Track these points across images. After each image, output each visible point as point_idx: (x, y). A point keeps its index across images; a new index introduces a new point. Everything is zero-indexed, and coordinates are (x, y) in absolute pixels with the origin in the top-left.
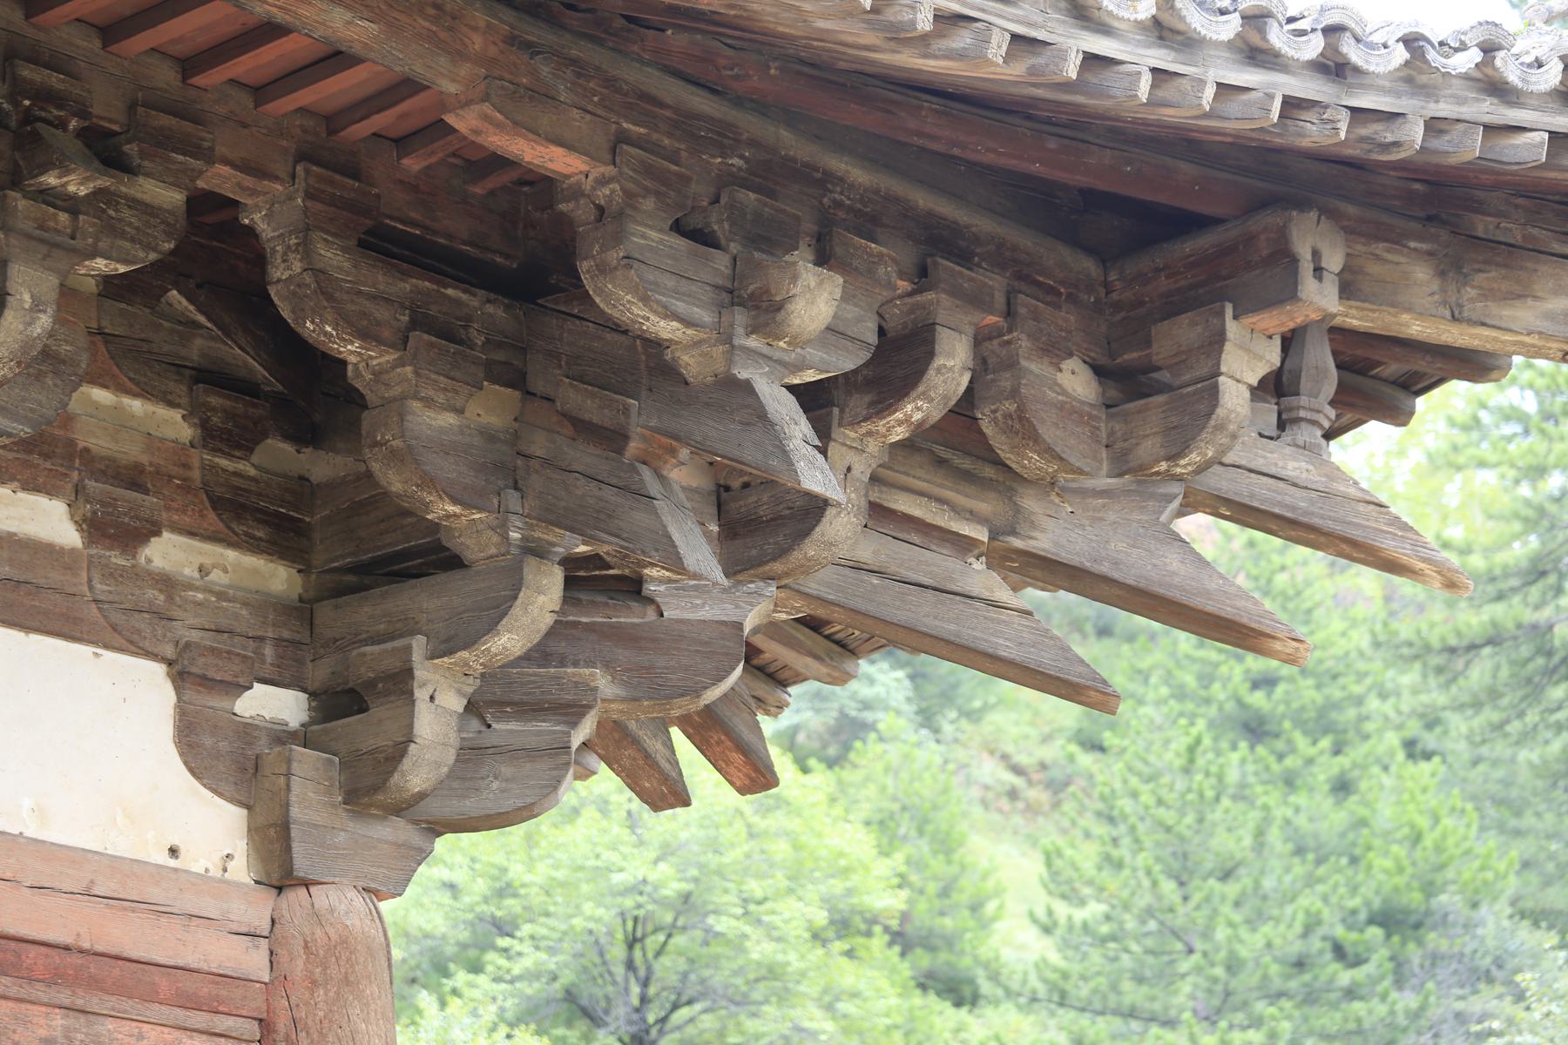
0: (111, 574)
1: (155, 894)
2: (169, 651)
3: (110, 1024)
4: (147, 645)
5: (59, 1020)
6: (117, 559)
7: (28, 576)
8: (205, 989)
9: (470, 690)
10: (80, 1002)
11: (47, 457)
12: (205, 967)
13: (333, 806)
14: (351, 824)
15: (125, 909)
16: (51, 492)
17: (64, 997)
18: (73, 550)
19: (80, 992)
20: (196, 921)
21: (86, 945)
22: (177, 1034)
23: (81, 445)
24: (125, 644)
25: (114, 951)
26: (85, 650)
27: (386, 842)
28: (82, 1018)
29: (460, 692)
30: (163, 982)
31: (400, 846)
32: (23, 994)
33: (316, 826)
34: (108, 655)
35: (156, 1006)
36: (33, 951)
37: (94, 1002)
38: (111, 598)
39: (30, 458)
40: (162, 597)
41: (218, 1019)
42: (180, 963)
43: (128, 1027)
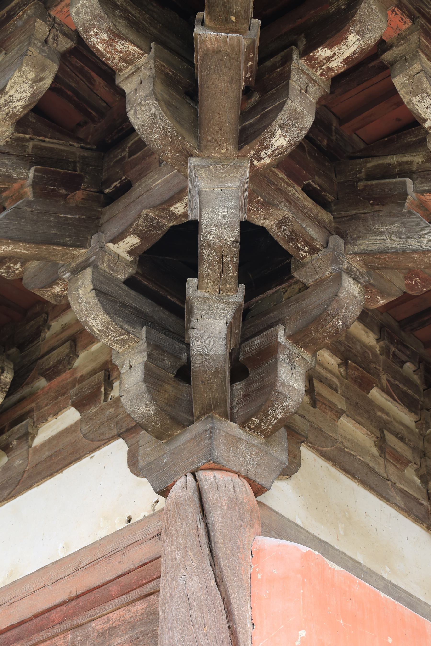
0: (91, 419)
1: (110, 547)
2: (115, 432)
3: (93, 624)
4: (107, 436)
5: (70, 636)
6: (93, 410)
7: (57, 449)
8: (133, 576)
9: (145, 345)
10: (75, 623)
11: (63, 394)
12: (132, 567)
13: (159, 446)
14: (168, 448)
15: (94, 565)
16: (65, 407)
17: (67, 625)
18: (76, 424)
19: (75, 618)
20: (129, 548)
21: (74, 595)
22: (127, 608)
23: (79, 376)
24: (99, 443)
25: (86, 589)
26: (86, 460)
27: (187, 442)
28: (80, 629)
29: (140, 352)
30: (114, 589)
31: (195, 438)
32: (49, 634)
33: (151, 463)
34: (96, 454)
35: (112, 602)
36: (54, 612)
37: (82, 619)
38: (90, 429)
39: (58, 400)
40: (113, 410)
41: (143, 589)
42: (120, 573)
43: (102, 620)
